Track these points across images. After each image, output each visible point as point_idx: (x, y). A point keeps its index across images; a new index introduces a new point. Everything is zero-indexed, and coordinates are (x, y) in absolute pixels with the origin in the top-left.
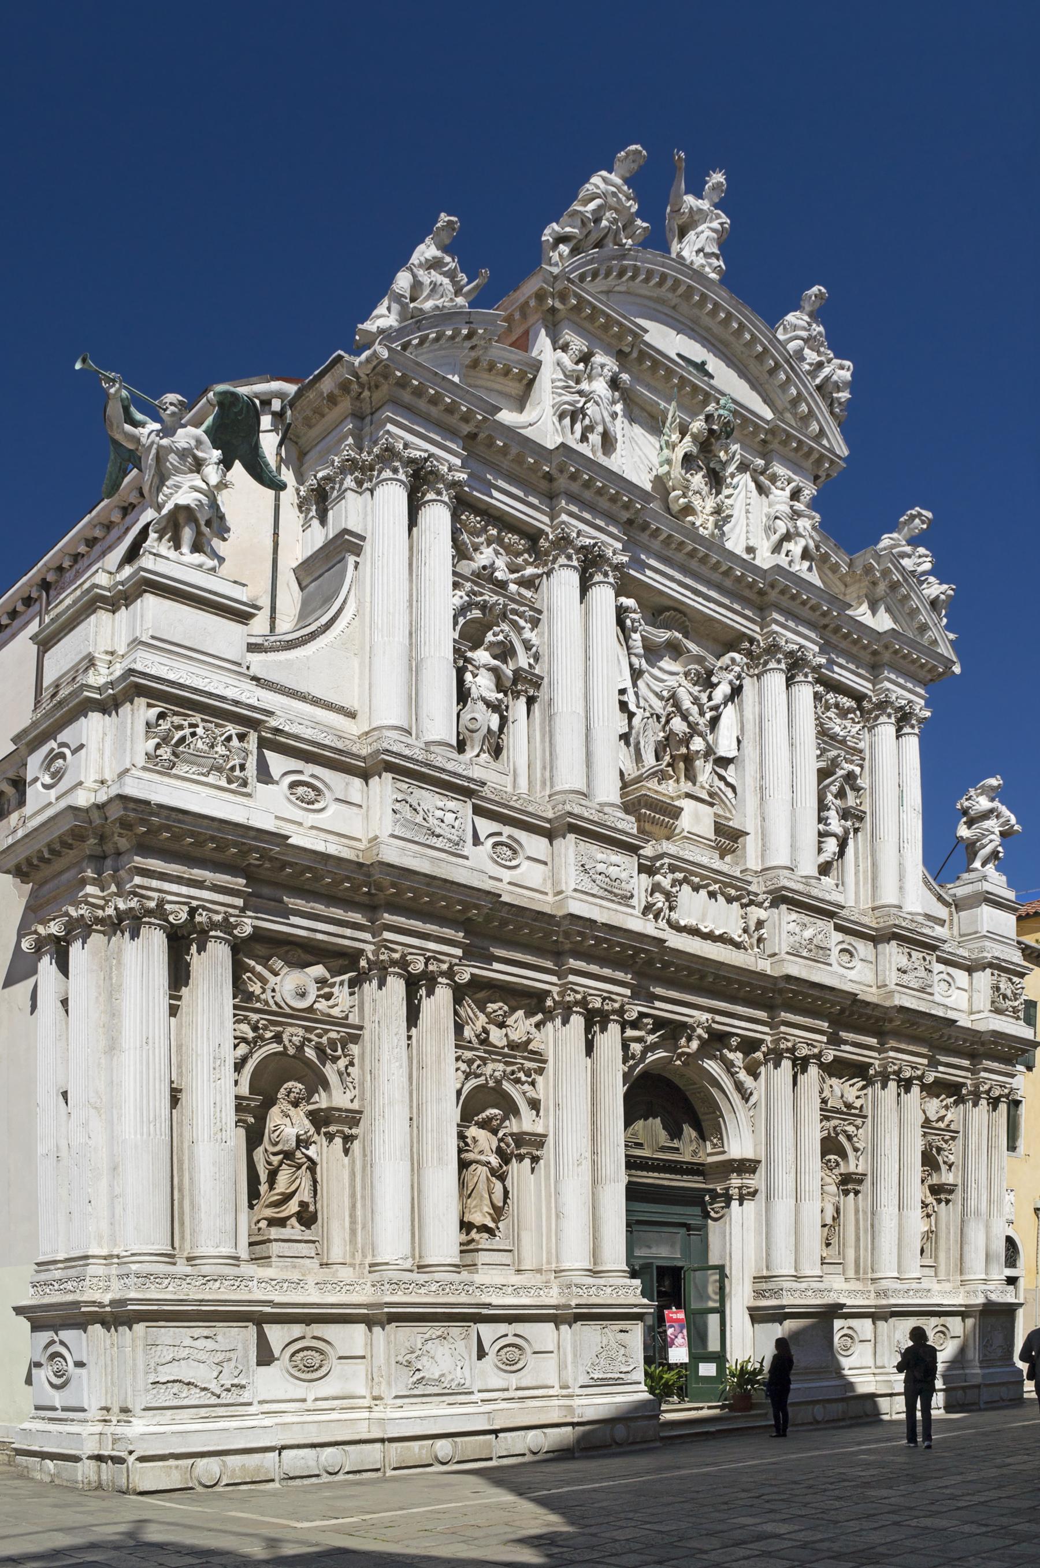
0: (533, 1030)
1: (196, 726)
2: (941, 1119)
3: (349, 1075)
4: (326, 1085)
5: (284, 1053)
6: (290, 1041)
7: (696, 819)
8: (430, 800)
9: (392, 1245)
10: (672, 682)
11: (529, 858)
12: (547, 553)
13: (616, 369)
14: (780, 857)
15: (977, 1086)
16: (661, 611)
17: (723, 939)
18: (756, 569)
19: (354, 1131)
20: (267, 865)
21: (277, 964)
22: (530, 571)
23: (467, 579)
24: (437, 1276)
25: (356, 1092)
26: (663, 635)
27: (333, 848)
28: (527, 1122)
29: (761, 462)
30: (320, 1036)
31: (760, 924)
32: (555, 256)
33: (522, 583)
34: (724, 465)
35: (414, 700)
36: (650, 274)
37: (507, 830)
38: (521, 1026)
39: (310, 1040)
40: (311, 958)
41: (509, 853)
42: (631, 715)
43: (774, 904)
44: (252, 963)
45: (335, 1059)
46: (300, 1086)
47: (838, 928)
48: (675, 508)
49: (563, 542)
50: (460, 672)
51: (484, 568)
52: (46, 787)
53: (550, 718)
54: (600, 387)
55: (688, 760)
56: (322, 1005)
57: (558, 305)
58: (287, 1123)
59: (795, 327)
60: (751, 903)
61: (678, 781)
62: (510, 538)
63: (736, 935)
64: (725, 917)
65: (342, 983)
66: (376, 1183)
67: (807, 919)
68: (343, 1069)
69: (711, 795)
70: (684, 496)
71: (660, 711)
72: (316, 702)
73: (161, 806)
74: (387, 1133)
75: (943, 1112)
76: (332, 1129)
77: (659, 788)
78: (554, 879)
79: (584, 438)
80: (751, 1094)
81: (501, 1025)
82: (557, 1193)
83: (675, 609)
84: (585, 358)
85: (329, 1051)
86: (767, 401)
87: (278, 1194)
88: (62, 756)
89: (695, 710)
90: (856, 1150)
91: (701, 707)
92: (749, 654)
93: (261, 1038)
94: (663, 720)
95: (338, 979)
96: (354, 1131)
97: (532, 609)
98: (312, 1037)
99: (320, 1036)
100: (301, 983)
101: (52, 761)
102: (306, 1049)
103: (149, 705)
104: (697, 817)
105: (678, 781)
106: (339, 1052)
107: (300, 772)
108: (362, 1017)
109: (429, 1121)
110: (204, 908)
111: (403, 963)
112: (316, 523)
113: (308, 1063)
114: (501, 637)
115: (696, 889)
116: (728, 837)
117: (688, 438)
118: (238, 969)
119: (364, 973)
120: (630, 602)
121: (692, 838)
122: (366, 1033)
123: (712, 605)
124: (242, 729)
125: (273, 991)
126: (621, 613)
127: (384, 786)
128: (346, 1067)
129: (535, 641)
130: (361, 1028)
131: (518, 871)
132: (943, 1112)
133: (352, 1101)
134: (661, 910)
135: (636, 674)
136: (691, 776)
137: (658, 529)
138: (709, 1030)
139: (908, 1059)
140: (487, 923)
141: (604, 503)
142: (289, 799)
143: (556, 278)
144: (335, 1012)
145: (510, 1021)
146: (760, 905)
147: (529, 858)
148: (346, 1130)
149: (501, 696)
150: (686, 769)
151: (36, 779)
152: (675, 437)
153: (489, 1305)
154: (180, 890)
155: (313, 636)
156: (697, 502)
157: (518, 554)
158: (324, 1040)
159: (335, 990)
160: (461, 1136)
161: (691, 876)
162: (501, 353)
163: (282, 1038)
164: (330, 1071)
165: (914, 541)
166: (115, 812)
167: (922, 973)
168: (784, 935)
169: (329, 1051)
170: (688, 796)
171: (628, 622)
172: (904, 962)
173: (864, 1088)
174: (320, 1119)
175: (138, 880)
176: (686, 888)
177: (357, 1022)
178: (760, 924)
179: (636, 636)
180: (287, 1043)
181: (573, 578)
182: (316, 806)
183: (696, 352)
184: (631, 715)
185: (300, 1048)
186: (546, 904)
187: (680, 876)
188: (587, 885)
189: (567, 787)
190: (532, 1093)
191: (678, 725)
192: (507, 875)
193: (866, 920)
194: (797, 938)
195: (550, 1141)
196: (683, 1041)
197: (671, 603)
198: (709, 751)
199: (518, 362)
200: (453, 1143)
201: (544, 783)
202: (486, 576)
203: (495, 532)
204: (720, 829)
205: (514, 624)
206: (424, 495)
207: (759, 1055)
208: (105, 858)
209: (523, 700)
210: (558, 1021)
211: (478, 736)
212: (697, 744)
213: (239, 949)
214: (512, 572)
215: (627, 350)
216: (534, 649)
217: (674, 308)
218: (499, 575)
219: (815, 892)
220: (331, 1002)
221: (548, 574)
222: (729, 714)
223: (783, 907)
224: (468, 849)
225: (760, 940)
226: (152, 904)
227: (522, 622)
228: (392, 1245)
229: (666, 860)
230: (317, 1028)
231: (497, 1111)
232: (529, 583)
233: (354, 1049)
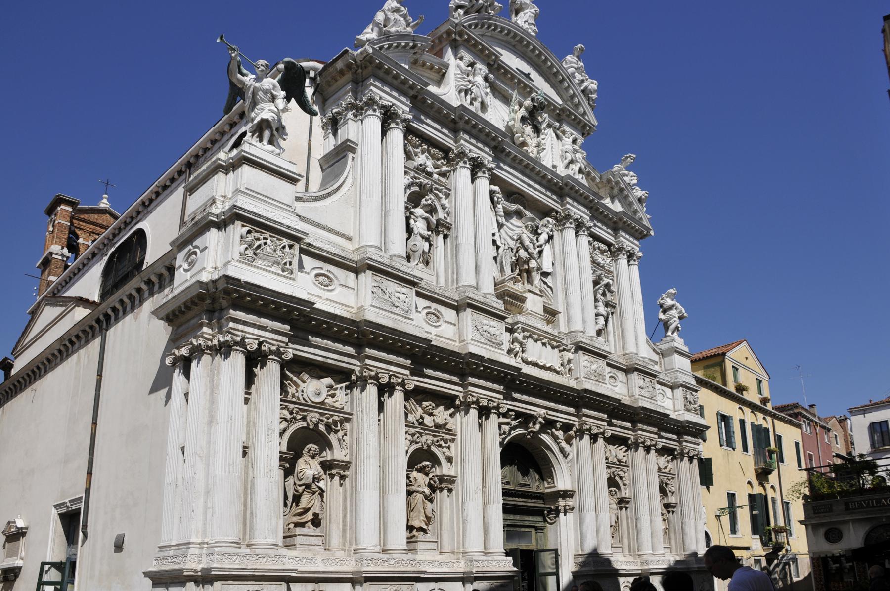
1: (267, 239)
2: (666, 468)
4: (330, 447)
5: (307, 428)
7: (534, 304)
9: (368, 539)
10: (518, 231)
11: (446, 322)
12: (453, 160)
14: (577, 326)
15: (682, 450)
17: (550, 369)
18: (558, 176)
19: (346, 473)
20: (302, 319)
21: (305, 376)
22: (444, 168)
23: (412, 170)
24: (394, 556)
25: (348, 451)
27: (338, 311)
29: (558, 124)
30: (328, 418)
31: (569, 361)
32: (456, 15)
34: (541, 123)
35: (384, 232)
36: (503, 29)
37: (434, 306)
39: (322, 421)
40: (324, 374)
41: (435, 318)
42: (498, 247)
43: (576, 351)
44: (291, 375)
45: (336, 432)
47: (609, 365)
48: (518, 142)
49: (462, 155)
50: (408, 219)
51: (421, 165)
52: (186, 271)
53: (456, 246)
55: (529, 272)
56: (330, 401)
57: (458, 38)
58: (308, 467)
59: (571, 62)
60: (564, 350)
61: (523, 283)
62: (434, 151)
63: (557, 367)
64: (550, 357)
65: (341, 388)
66: (359, 503)
69: (541, 291)
70: (522, 136)
71: (512, 246)
72: (330, 230)
73: (246, 283)
74: (367, 474)
75: (666, 464)
76: (334, 472)
77: (514, 287)
78: (460, 333)
79: (471, 104)
82: (463, 509)
83: (519, 194)
86: (558, 94)
88: (195, 253)
89: (531, 246)
91: (534, 244)
93: (294, 418)
95: (339, 386)
96: (346, 473)
97: (446, 188)
99: (328, 418)
100: (318, 388)
101: (190, 256)
104: (534, 303)
105: (523, 283)
106: (339, 428)
108: (352, 408)
109: (390, 468)
110: (267, 342)
111: (376, 378)
112: (331, 136)
113: (321, 433)
114: (429, 202)
116: (551, 314)
117: (523, 109)
118: (284, 377)
121: (532, 314)
122: (354, 417)
124: (291, 242)
126: (492, 193)
127: (367, 278)
129: (447, 205)
130: (351, 414)
131: (440, 328)
132: (666, 464)
134: (517, 352)
135: (500, 226)
136: (530, 280)
138: (545, 418)
139: (646, 434)
140: (422, 355)
141: (482, 137)
143: (457, 25)
144: (337, 405)
145: (435, 412)
146: (569, 351)
147: (446, 322)
148: (342, 472)
149: (430, 233)
150: (528, 277)
151: (180, 267)
152: (517, 107)
154: (253, 330)
155: (329, 194)
156: (528, 140)
157: (438, 159)
158: (330, 420)
159: (337, 392)
160: (408, 477)
161: (533, 334)
162: (429, 58)
165: (628, 169)
166: (221, 285)
168: (582, 368)
170: (530, 291)
171: (496, 198)
173: (626, 451)
174: (327, 466)
175: (231, 324)
176: (530, 340)
177: (349, 411)
178: (569, 361)
179: (500, 206)
181: (468, 173)
183: (526, 68)
184: (498, 247)
185: (316, 425)
186: (455, 347)
187: (527, 334)
188: (478, 337)
189: (466, 283)
192: (434, 331)
193: (621, 361)
195: (459, 479)
196: (531, 424)
197: (516, 190)
198: (539, 269)
199: (438, 63)
200: (404, 481)
201: (453, 281)
202: (421, 169)
203: (426, 147)
204: (546, 310)
205: (436, 195)
206: (389, 124)
208: (214, 312)
209: (441, 236)
210: (462, 413)
211: (418, 254)
212: (533, 264)
213: (285, 365)
214: (435, 168)
215: (492, 63)
217: (514, 46)
218: (428, 169)
219: (596, 345)
221: (454, 171)
222: (547, 249)
223: (581, 352)
224: (413, 315)
225: (569, 370)
226: (238, 339)
227: (440, 195)
228: (368, 539)
229: (519, 325)
232: (443, 175)
233: (347, 426)
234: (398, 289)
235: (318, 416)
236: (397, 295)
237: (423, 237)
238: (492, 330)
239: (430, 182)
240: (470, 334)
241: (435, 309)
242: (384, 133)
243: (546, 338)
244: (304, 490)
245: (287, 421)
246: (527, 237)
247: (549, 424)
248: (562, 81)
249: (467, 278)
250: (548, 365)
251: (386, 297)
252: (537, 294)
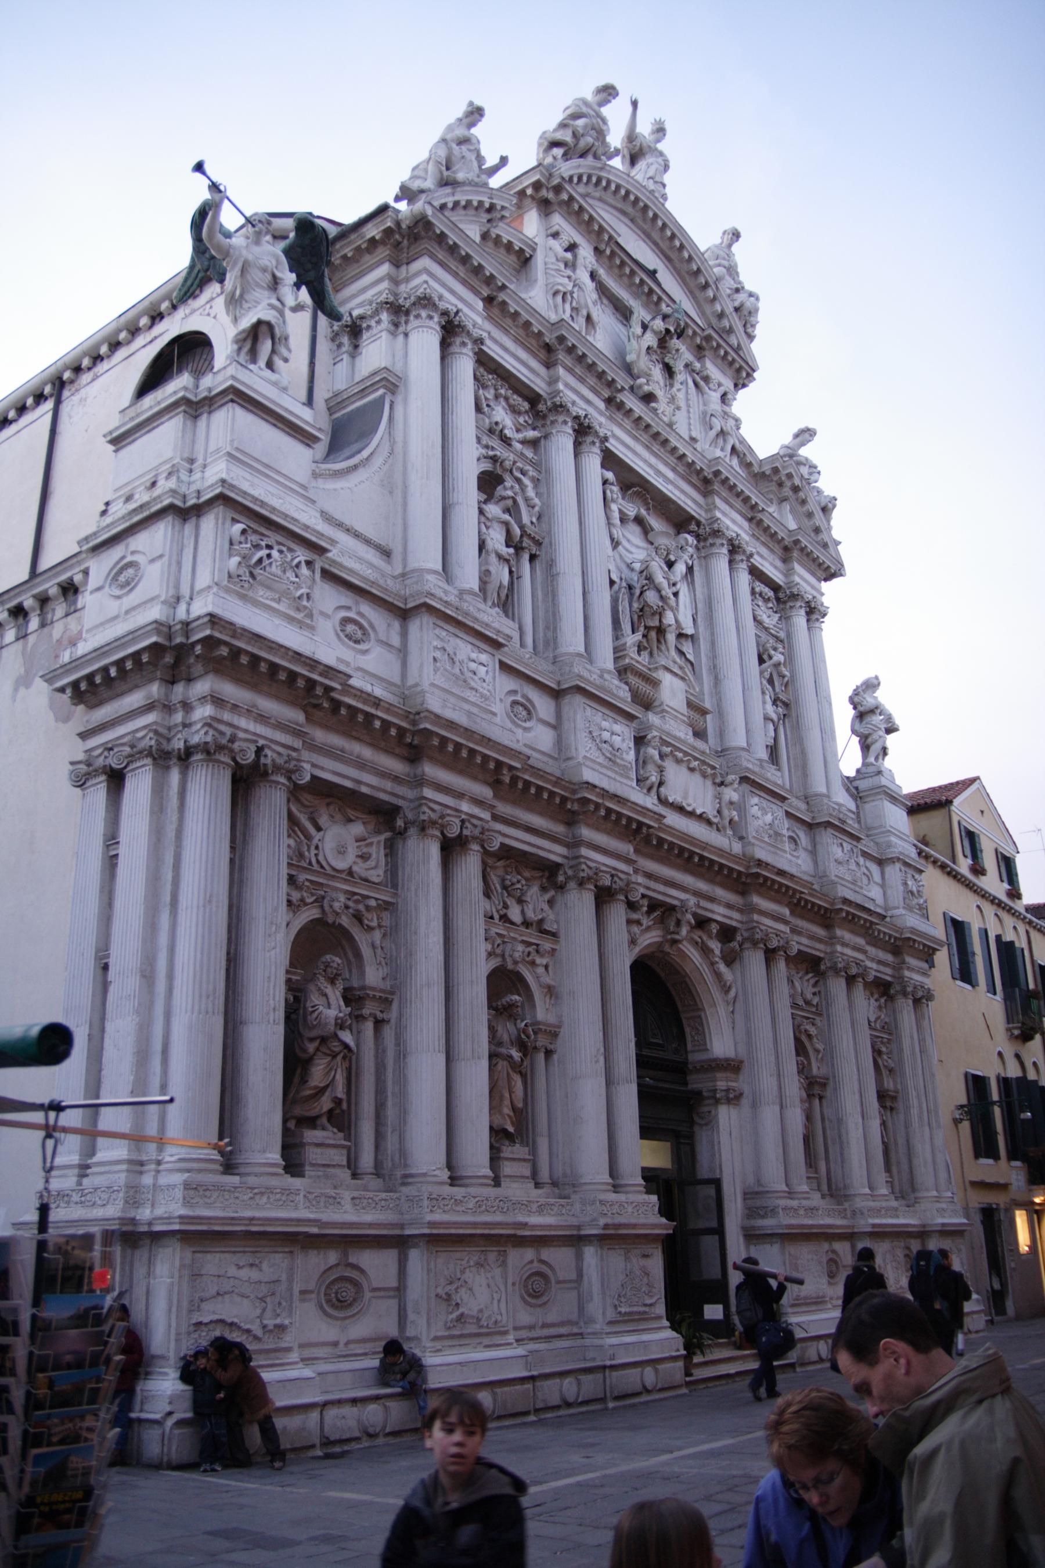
0: (546, 907)
7: (672, 692)
8: (464, 649)
13: (594, 261)
16: (631, 483)
17: (702, 818)
26: (631, 511)
28: (543, 1012)
33: (523, 442)
38: (536, 903)
41: (524, 713)
46: (337, 960)
49: (559, 408)
51: (497, 423)
54: (584, 277)
55: (661, 631)
56: (359, 869)
63: (711, 814)
65: (379, 842)
67: (765, 803)
70: (648, 384)
80: (730, 988)
81: (520, 901)
84: (572, 248)
89: (665, 584)
90: (817, 1051)
92: (698, 537)
94: (637, 592)
95: (375, 840)
98: (351, 904)
103: (234, 521)
107: (348, 608)
114: (510, 493)
115: (678, 761)
119: (400, 833)
120: (610, 475)
123: (670, 487)
125: (317, 848)
129: (537, 501)
137: (631, 410)
142: (338, 635)
149: (511, 550)
152: (639, 330)
153: (525, 1225)
157: (519, 413)
159: (373, 850)
167: (853, 867)
168: (749, 819)
172: (838, 853)
179: (614, 507)
180: (327, 908)
182: (362, 647)
190: (547, 980)
191: (651, 597)
194: (760, 822)
204: (690, 704)
205: (518, 481)
207: (734, 944)
214: (518, 431)
216: (537, 509)
218: (508, 432)
220: (371, 863)
221: (546, 437)
227: (526, 481)
231: (517, 997)
234: (474, 656)
236: (473, 666)
237: (500, 557)
238: (617, 740)
239: (512, 457)
240: (583, 748)
241: (524, 696)
242: (444, 356)
243: (696, 759)
244: (318, 1049)
246: (657, 569)
247: (702, 923)
248: (706, 286)
249: (572, 640)
250: (698, 812)
251: (457, 671)
252: (676, 675)
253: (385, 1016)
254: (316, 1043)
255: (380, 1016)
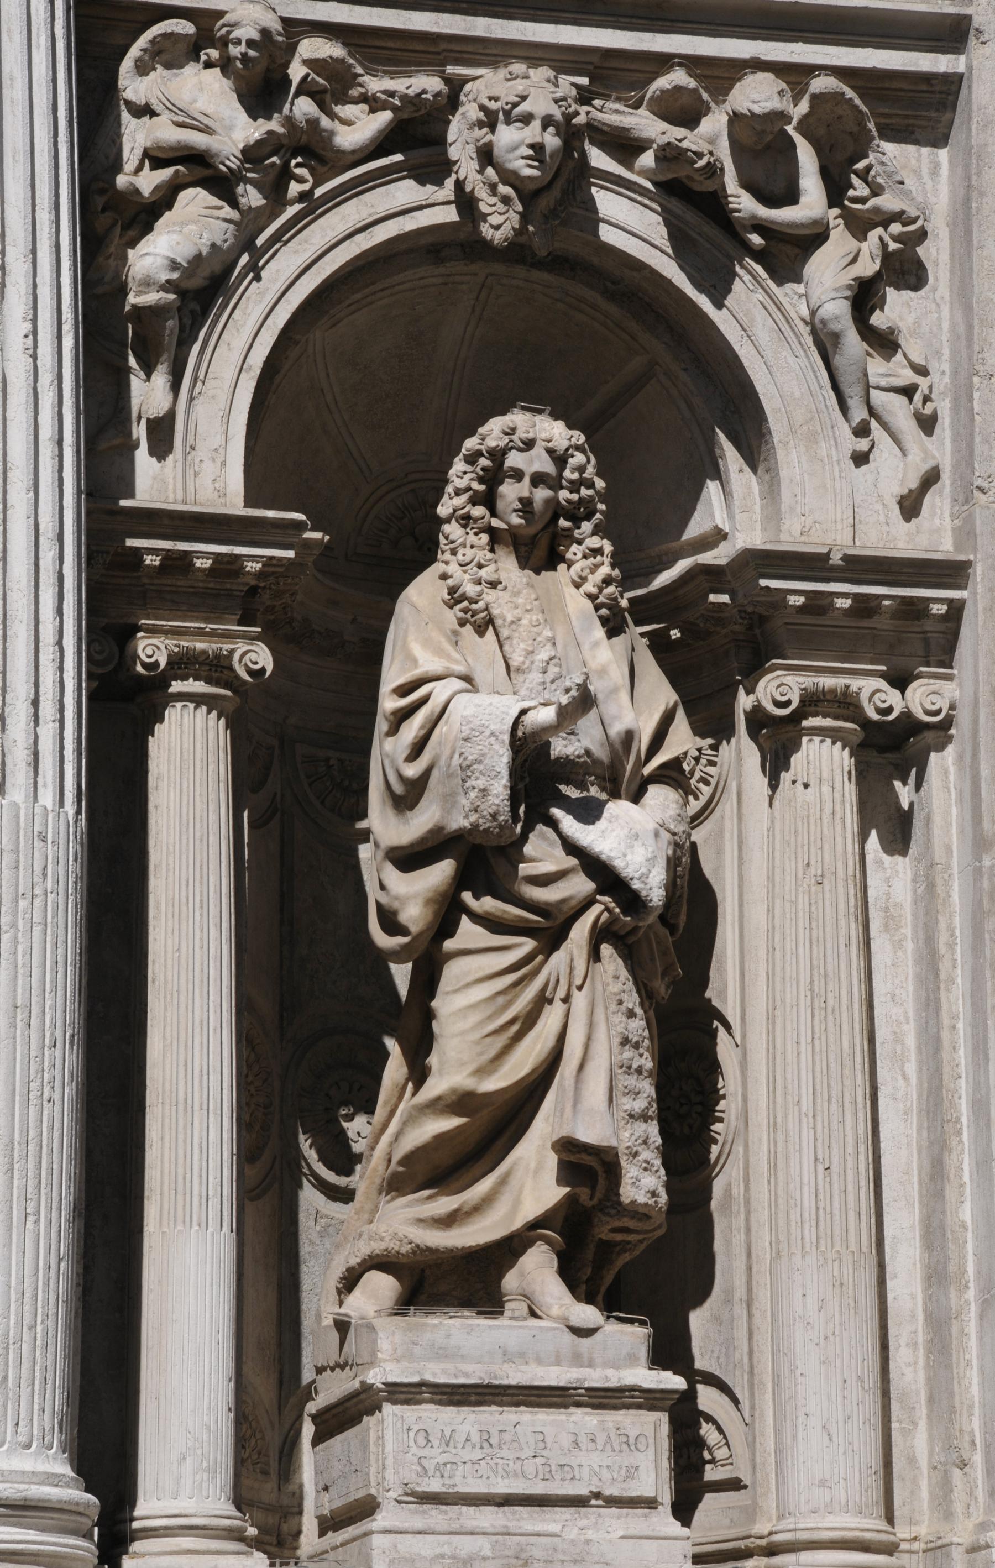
3: (885, 343)
6: (486, 156)
25: (940, 450)
39: (625, 146)
45: (787, 254)
68: (837, 310)
85: (744, 203)
87: (439, 1106)
93: (312, 148)
99: (684, 112)
102: (607, 203)
128: (864, 297)
133: (910, 506)
158: (711, 135)
163: (441, 142)
164: (759, 325)
169: (744, 203)
185: (559, 191)
230: (665, 62)
235: (543, 92)
245: (222, 185)
253: (922, 698)
254: (441, 872)
255: (873, 692)
